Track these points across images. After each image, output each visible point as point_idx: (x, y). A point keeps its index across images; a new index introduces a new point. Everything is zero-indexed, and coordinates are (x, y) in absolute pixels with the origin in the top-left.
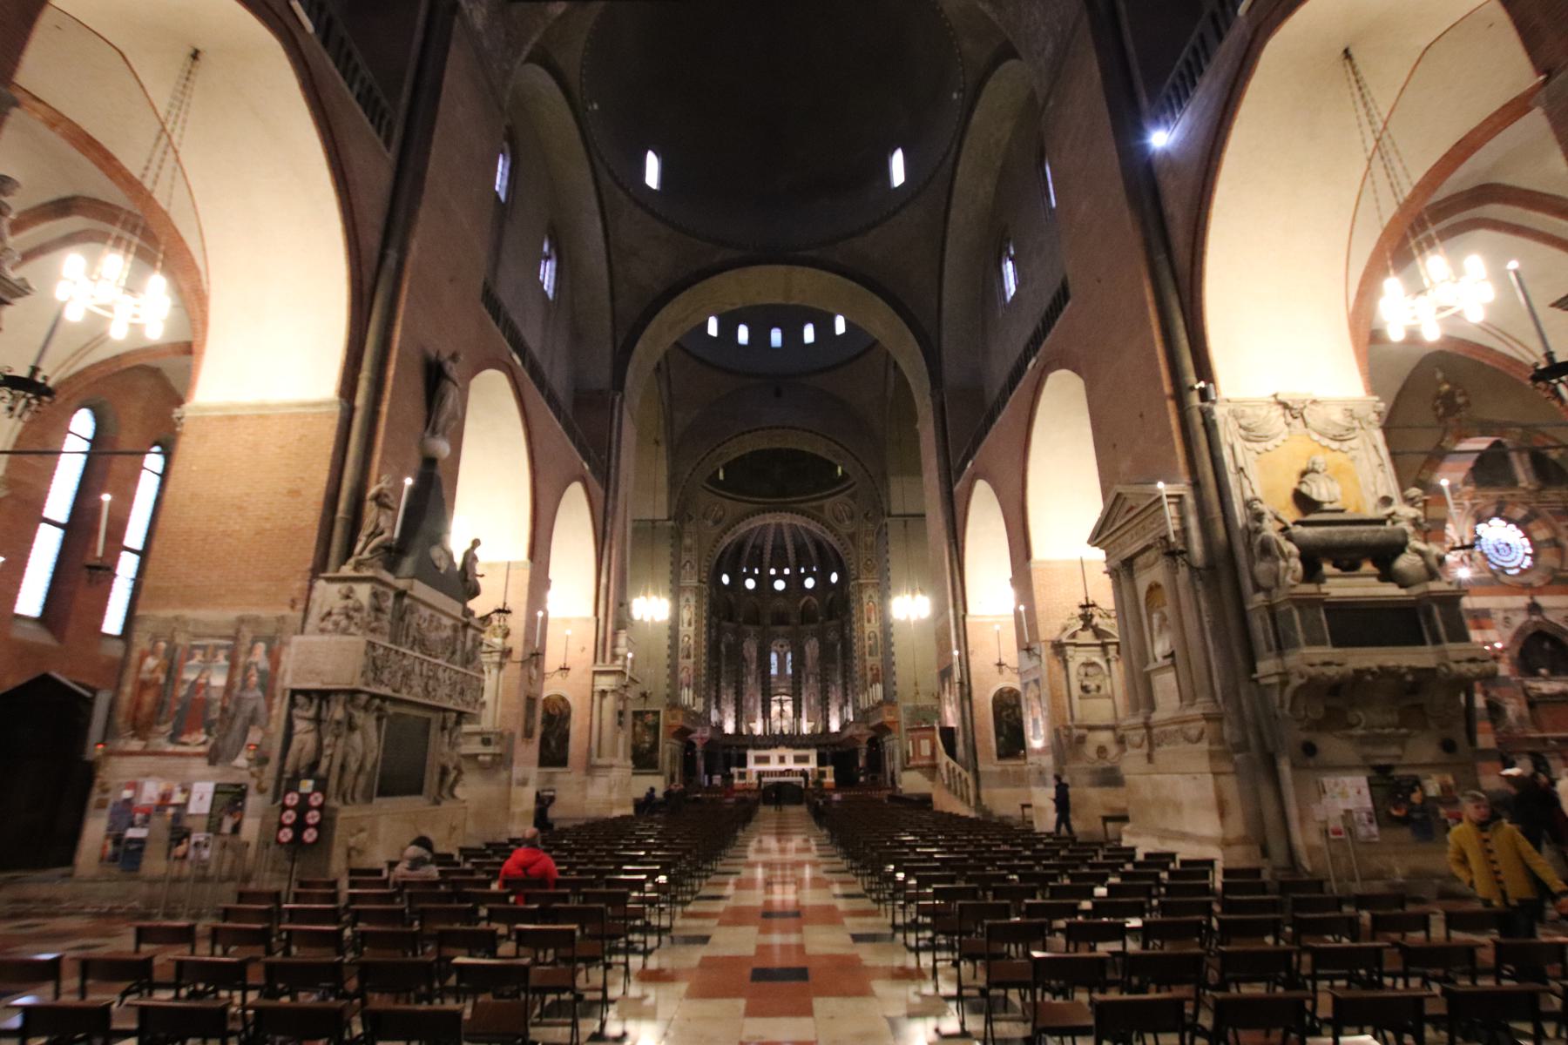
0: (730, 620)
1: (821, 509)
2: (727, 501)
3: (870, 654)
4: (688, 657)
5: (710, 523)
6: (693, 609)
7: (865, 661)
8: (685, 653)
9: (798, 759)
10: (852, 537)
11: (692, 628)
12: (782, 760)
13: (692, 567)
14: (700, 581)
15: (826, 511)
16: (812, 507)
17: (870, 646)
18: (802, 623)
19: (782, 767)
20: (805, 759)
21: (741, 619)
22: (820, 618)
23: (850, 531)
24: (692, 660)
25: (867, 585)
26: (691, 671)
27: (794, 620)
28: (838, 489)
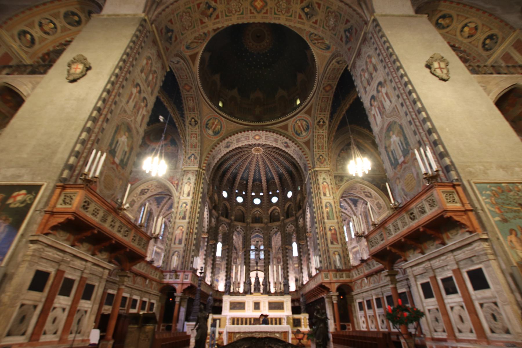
0: (227, 217)
1: (286, 128)
2: (223, 119)
3: (328, 218)
4: (184, 218)
5: (211, 132)
6: (192, 185)
7: (324, 223)
8: (182, 215)
9: (273, 306)
10: (307, 143)
11: (191, 197)
12: (257, 306)
13: (196, 158)
14: (200, 167)
15: (290, 129)
16: (280, 127)
17: (328, 213)
18: (271, 222)
19: (257, 314)
20: (279, 306)
21: (233, 218)
22: (282, 218)
23: (306, 139)
24: (187, 220)
25: (321, 172)
26: (185, 229)
27: (265, 220)
28: (297, 111)
